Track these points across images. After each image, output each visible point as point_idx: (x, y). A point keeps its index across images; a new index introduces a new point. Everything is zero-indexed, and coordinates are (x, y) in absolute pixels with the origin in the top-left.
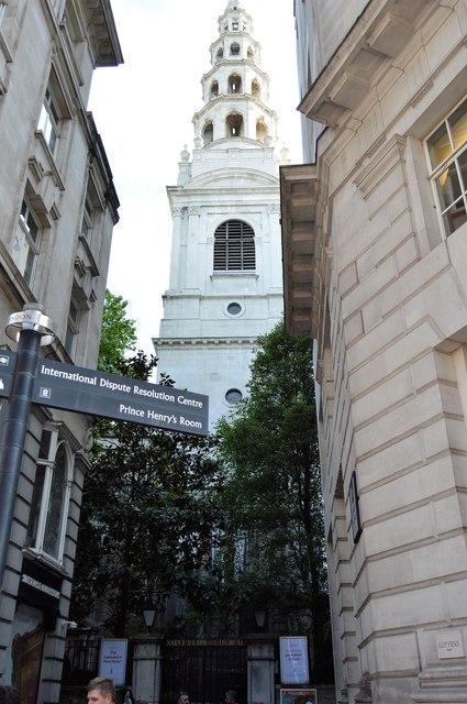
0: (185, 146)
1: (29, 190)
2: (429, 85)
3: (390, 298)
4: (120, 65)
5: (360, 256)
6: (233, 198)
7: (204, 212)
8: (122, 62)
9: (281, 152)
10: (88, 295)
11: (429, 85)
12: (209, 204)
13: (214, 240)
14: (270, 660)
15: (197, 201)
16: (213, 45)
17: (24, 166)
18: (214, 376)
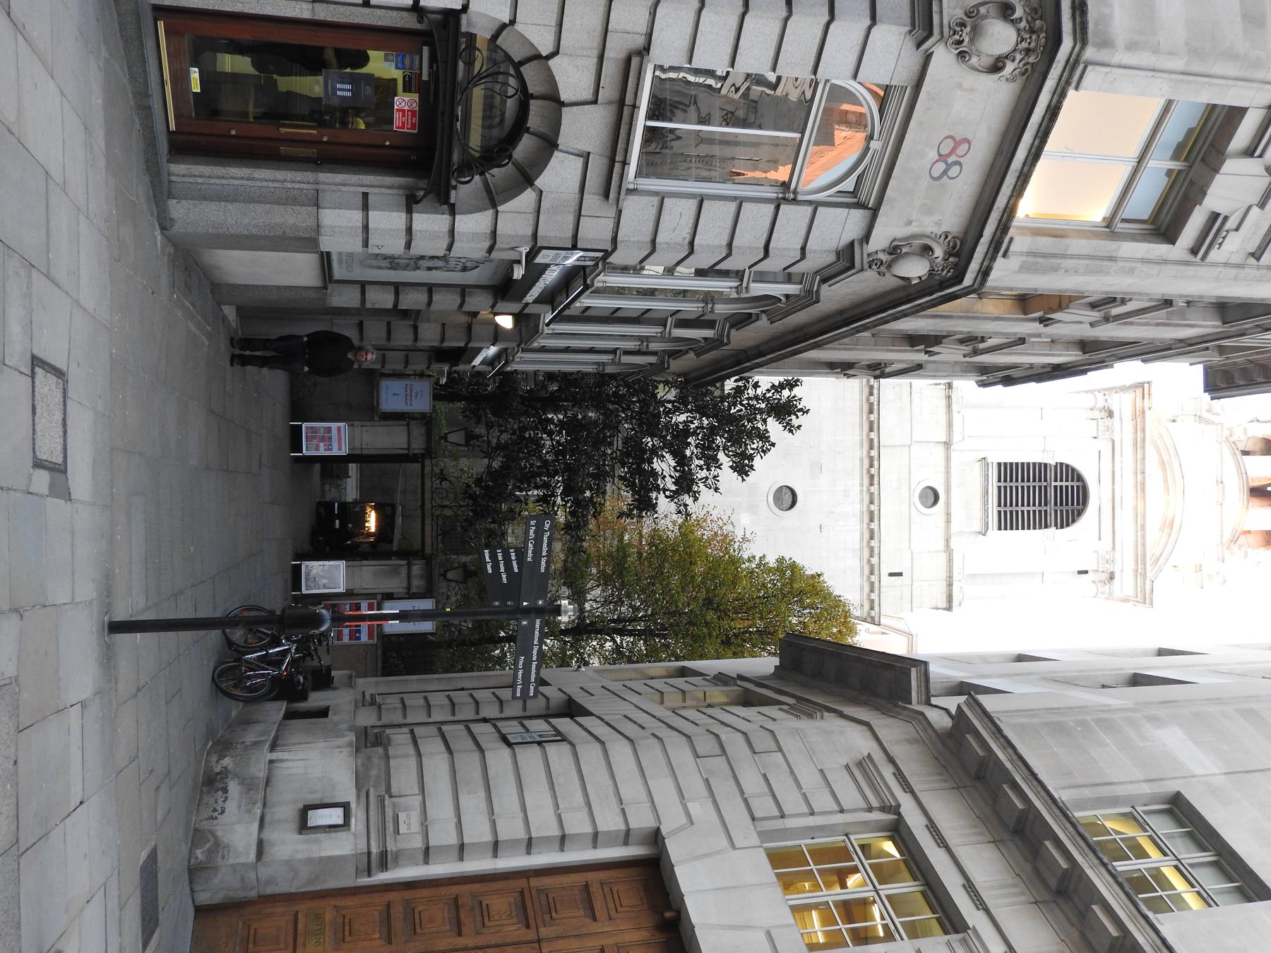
2: (942, 842)
3: (724, 788)
5: (785, 757)
11: (942, 842)
14: (409, 588)
18: (817, 468)
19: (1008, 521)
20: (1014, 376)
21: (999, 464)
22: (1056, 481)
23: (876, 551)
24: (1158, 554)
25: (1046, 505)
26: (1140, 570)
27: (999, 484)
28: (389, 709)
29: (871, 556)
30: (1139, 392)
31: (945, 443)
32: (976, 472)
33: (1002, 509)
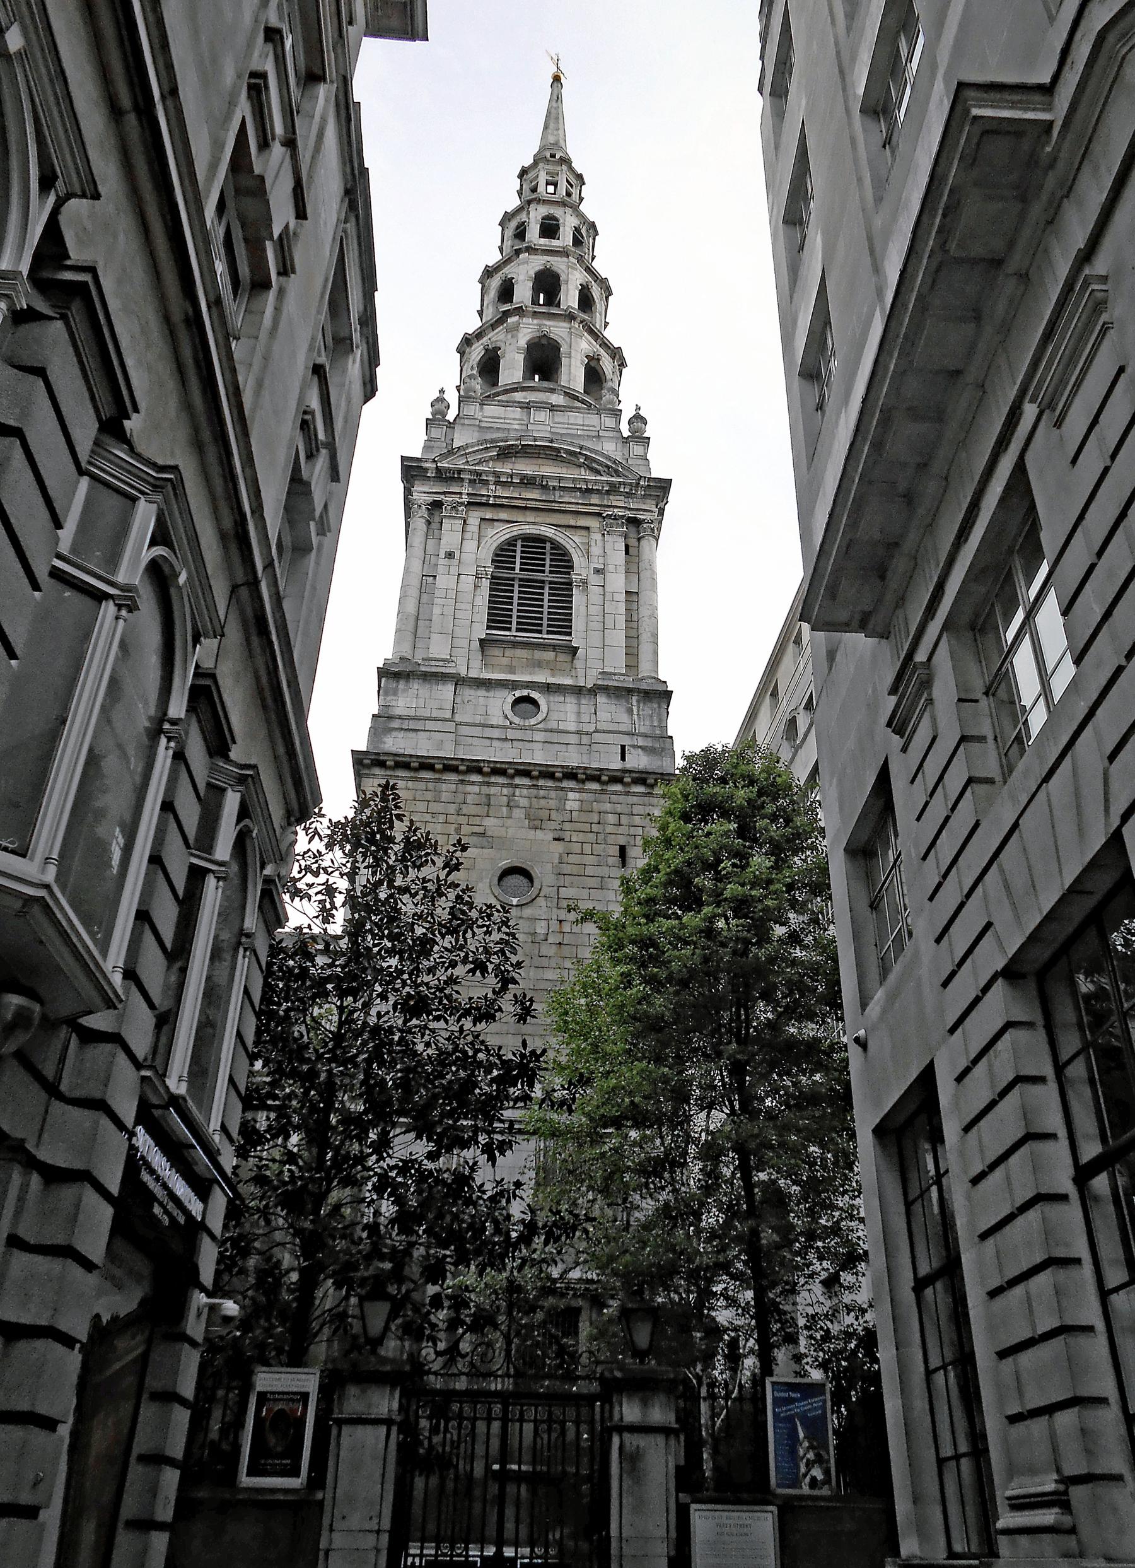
0: (442, 391)
1: (240, 161)
8: (426, 38)
9: (630, 423)
10: (319, 509)
16: (507, 218)
17: (239, 77)
20: (361, 308)
21: (489, 628)
22: (513, 569)
25: (543, 582)
27: (514, 626)
28: (1089, 1452)
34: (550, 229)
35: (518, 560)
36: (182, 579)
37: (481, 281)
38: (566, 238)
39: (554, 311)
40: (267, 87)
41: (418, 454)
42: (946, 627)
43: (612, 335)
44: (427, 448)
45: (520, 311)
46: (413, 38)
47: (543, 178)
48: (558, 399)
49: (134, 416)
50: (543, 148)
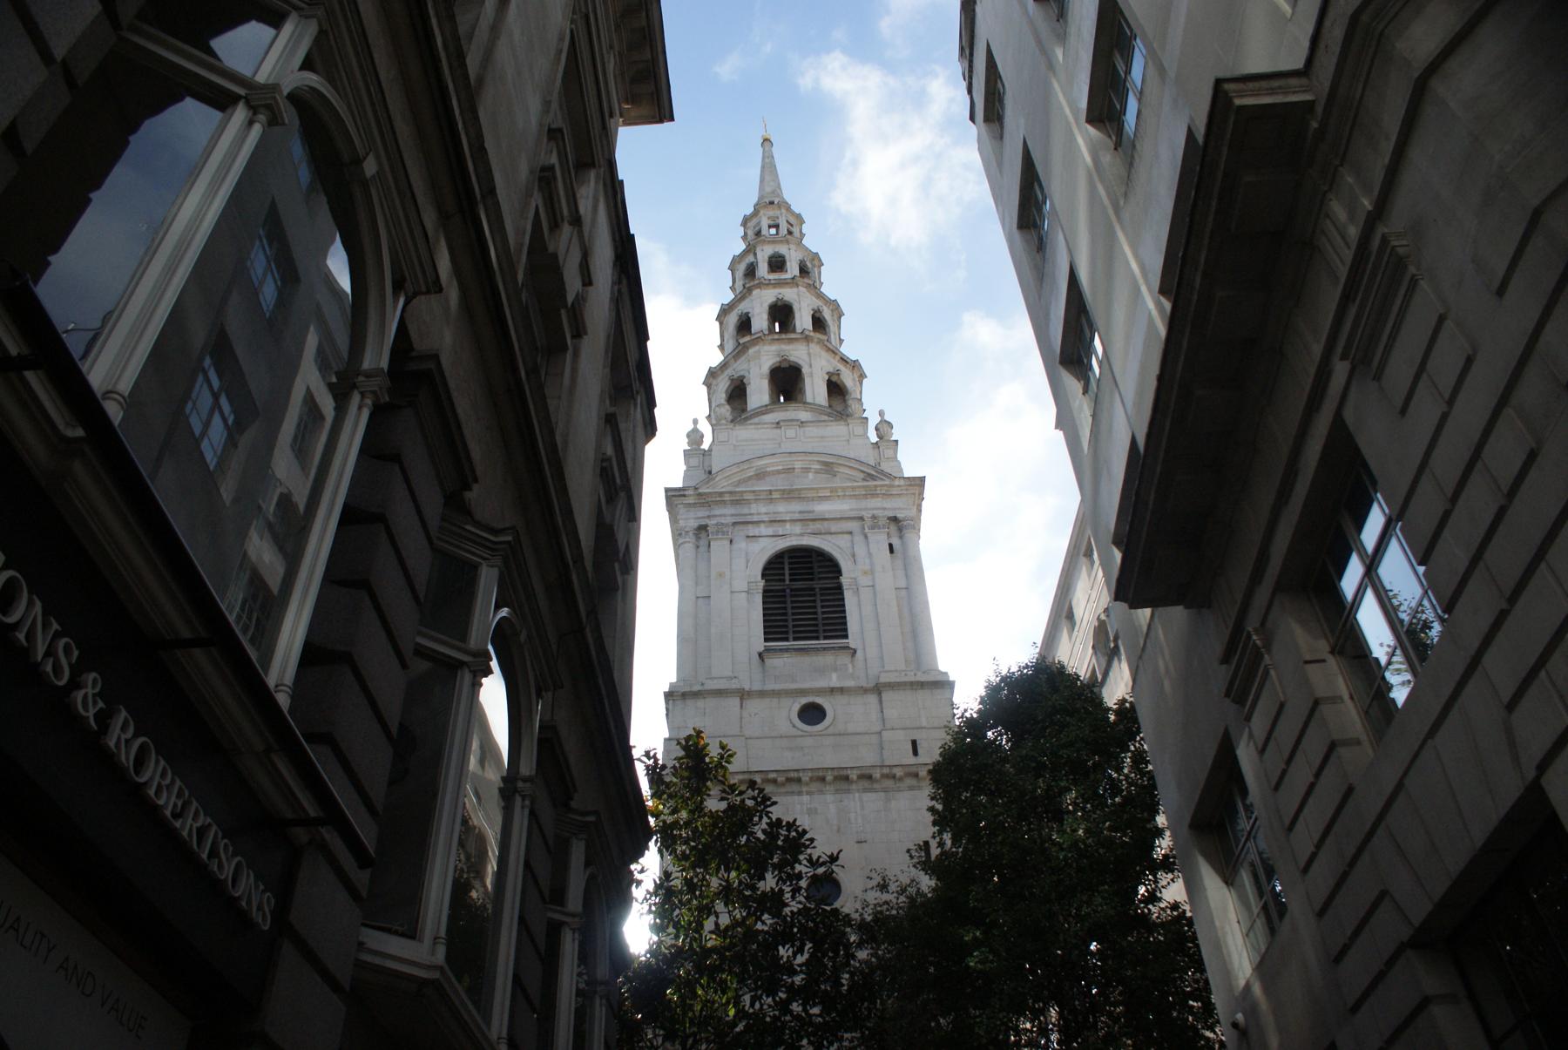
0: (695, 422)
4: (666, 125)
6: (796, 507)
7: (740, 533)
8: (672, 119)
9: (877, 429)
10: (622, 548)
12: (749, 518)
13: (762, 583)
15: (726, 514)
16: (736, 261)
17: (532, 172)
19: (836, 626)
21: (766, 640)
22: (784, 580)
23: (886, 771)
24: (862, 476)
25: (813, 589)
26: (883, 492)
29: (894, 777)
30: (677, 501)
31: (742, 699)
32: (777, 663)
33: (822, 635)
34: (777, 264)
35: (787, 572)
36: (523, 637)
37: (719, 318)
38: (793, 269)
39: (793, 336)
40: (555, 178)
41: (680, 485)
42: (1279, 588)
43: (847, 350)
44: (686, 476)
45: (758, 340)
46: (661, 121)
47: (765, 223)
48: (804, 415)
49: (475, 487)
50: (761, 198)
